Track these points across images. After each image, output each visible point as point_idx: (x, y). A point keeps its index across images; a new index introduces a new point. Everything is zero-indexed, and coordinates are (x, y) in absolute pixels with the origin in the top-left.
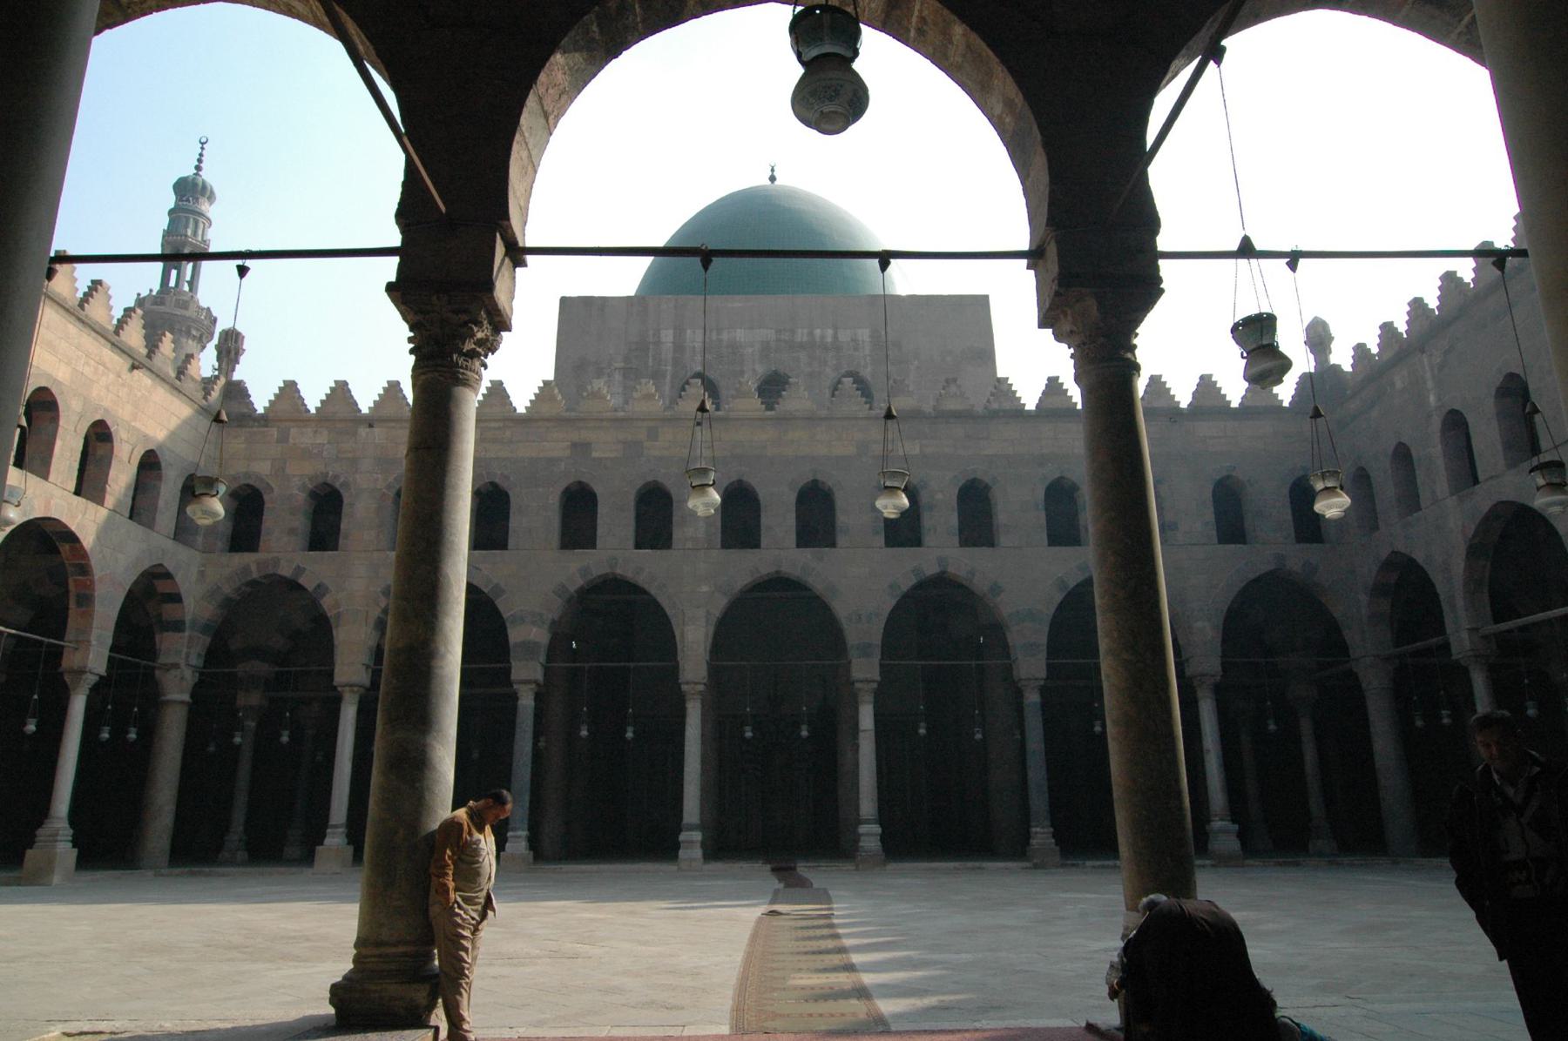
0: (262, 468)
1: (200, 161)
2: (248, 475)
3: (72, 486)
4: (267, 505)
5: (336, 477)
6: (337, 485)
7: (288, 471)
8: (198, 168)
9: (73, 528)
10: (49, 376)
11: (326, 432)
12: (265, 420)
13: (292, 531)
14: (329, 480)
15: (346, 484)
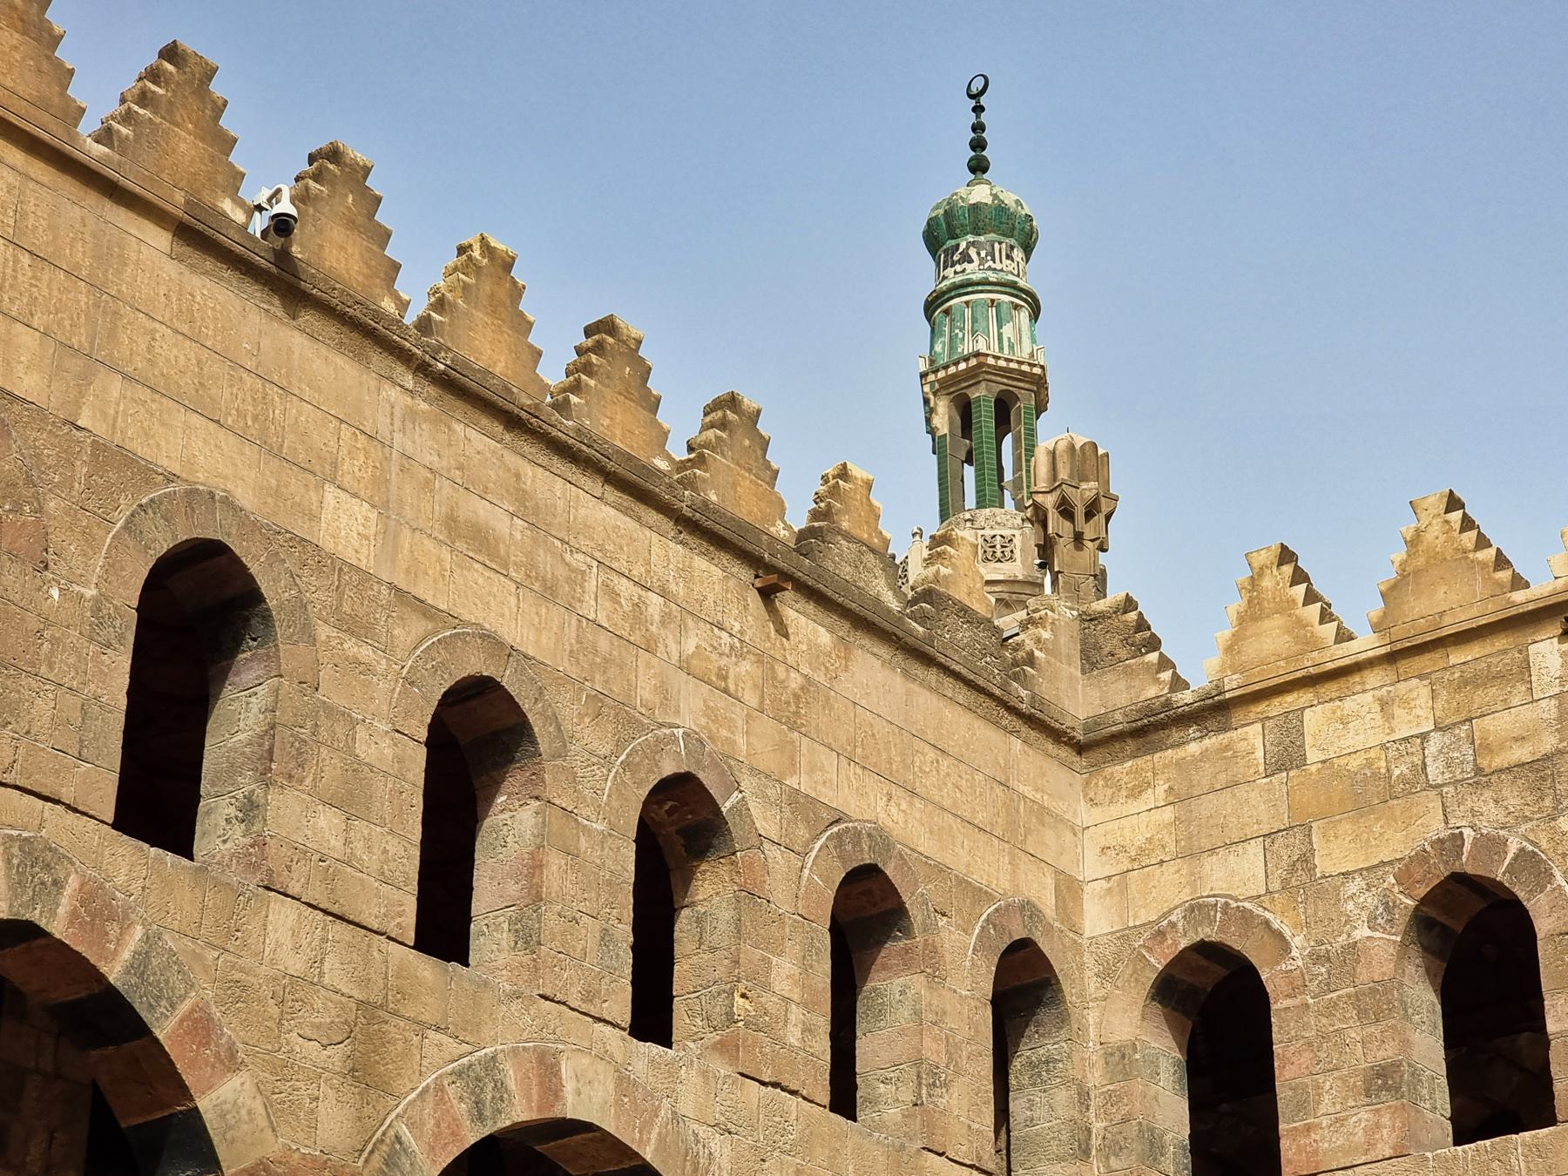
0: (1240, 875)
1: (978, 145)
2: (1197, 910)
3: (620, 1006)
4: (1279, 1005)
5: (1492, 845)
6: (1500, 874)
7: (1322, 865)
8: (978, 167)
9: (648, 1155)
10: (492, 642)
11: (1419, 691)
12: (1216, 711)
13: (1384, 1081)
14: (1467, 864)
15: (1529, 861)
